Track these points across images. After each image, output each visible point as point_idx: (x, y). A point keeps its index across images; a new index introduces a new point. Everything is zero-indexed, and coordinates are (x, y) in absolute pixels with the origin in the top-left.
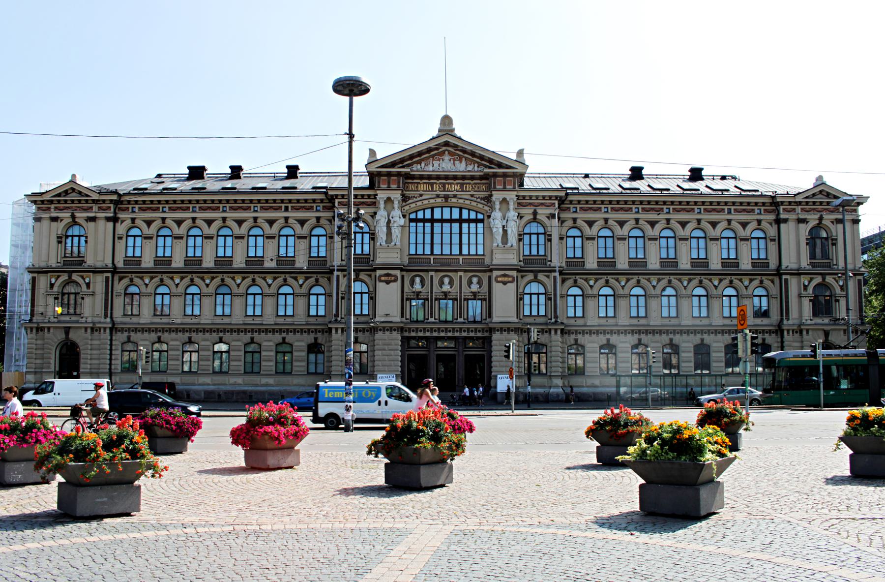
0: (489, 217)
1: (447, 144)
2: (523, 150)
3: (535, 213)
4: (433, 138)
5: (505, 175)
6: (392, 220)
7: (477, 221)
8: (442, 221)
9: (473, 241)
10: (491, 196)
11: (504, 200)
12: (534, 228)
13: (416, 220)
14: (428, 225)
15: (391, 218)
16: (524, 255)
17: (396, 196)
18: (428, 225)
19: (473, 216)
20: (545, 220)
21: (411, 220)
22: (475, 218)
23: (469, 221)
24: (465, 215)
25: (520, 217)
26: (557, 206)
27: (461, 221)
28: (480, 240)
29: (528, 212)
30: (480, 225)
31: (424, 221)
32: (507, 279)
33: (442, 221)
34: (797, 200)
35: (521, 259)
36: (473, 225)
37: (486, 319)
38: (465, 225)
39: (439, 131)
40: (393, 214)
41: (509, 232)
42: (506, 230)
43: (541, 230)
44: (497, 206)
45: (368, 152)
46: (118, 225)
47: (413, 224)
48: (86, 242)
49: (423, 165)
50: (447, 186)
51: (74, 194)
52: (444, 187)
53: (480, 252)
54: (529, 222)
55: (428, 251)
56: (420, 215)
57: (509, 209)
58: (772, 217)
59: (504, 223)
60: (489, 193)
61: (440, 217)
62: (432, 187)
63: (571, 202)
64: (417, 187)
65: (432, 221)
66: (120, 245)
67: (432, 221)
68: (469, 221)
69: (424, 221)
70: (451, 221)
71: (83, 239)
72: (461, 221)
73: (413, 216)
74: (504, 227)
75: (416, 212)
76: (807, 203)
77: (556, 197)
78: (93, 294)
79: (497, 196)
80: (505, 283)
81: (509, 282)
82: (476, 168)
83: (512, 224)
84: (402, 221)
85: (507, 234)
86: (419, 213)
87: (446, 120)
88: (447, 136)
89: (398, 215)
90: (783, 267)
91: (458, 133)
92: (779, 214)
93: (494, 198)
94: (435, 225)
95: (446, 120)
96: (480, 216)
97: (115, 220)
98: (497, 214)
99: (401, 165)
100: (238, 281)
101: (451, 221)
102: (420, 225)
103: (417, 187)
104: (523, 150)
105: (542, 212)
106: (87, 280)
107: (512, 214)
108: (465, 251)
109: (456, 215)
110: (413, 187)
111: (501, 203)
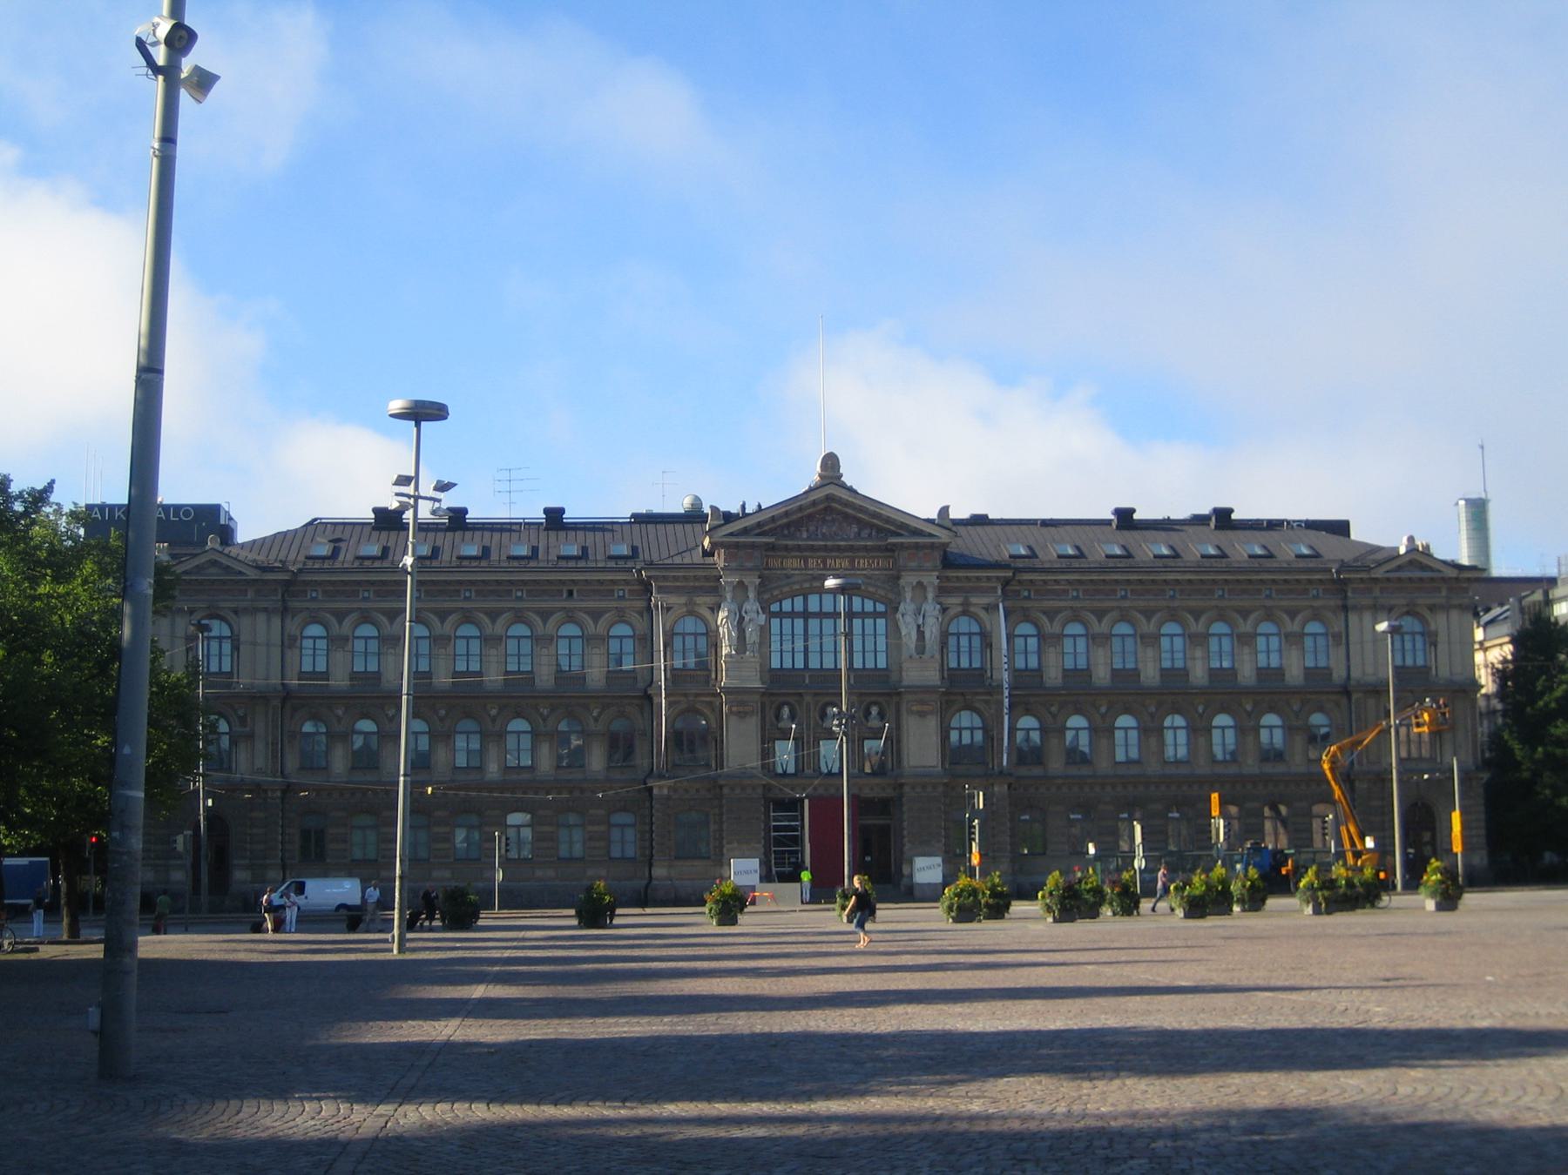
0: (897, 609)
1: (829, 498)
3: (966, 604)
4: (811, 490)
5: (917, 546)
6: (747, 618)
7: (875, 615)
8: (821, 615)
9: (869, 646)
10: (898, 578)
11: (920, 584)
12: (964, 624)
13: (781, 615)
15: (743, 614)
16: (949, 669)
17: (752, 581)
18: (799, 623)
19: (869, 606)
20: (983, 614)
21: (773, 615)
22: (872, 609)
23: (863, 615)
25: (944, 610)
26: (999, 592)
28: (881, 646)
29: (954, 601)
30: (881, 622)
31: (792, 615)
32: (926, 708)
33: (821, 615)
34: (1373, 576)
35: (946, 676)
36: (869, 622)
37: (892, 769)
38: (857, 622)
40: (747, 606)
41: (927, 635)
42: (923, 632)
43: (976, 629)
44: (908, 595)
46: (288, 621)
47: (775, 622)
48: (236, 648)
49: (792, 529)
50: (828, 561)
51: (213, 570)
52: (824, 563)
53: (882, 664)
54: (957, 616)
55: (800, 664)
57: (926, 598)
58: (1334, 602)
59: (920, 621)
60: (894, 572)
61: (817, 610)
62: (806, 562)
63: (1020, 582)
64: (782, 563)
65: (806, 615)
66: (292, 656)
67: (806, 615)
68: (863, 615)
69: (792, 615)
71: (227, 647)
73: (775, 607)
74: (919, 626)
76: (1388, 580)
77: (998, 578)
78: (251, 736)
79: (908, 580)
80: (922, 715)
83: (931, 621)
84: (762, 618)
85: (924, 637)
87: (831, 463)
88: (832, 486)
89: (755, 608)
90: (1353, 682)
91: (848, 479)
92: (1346, 597)
93: (902, 582)
94: (811, 621)
95: (831, 463)
96: (881, 608)
97: (285, 611)
98: (907, 607)
99: (757, 531)
100: (494, 712)
102: (787, 622)
103: (782, 563)
105: (978, 600)
106: (241, 713)
107: (931, 608)
110: (777, 563)
111: (913, 588)
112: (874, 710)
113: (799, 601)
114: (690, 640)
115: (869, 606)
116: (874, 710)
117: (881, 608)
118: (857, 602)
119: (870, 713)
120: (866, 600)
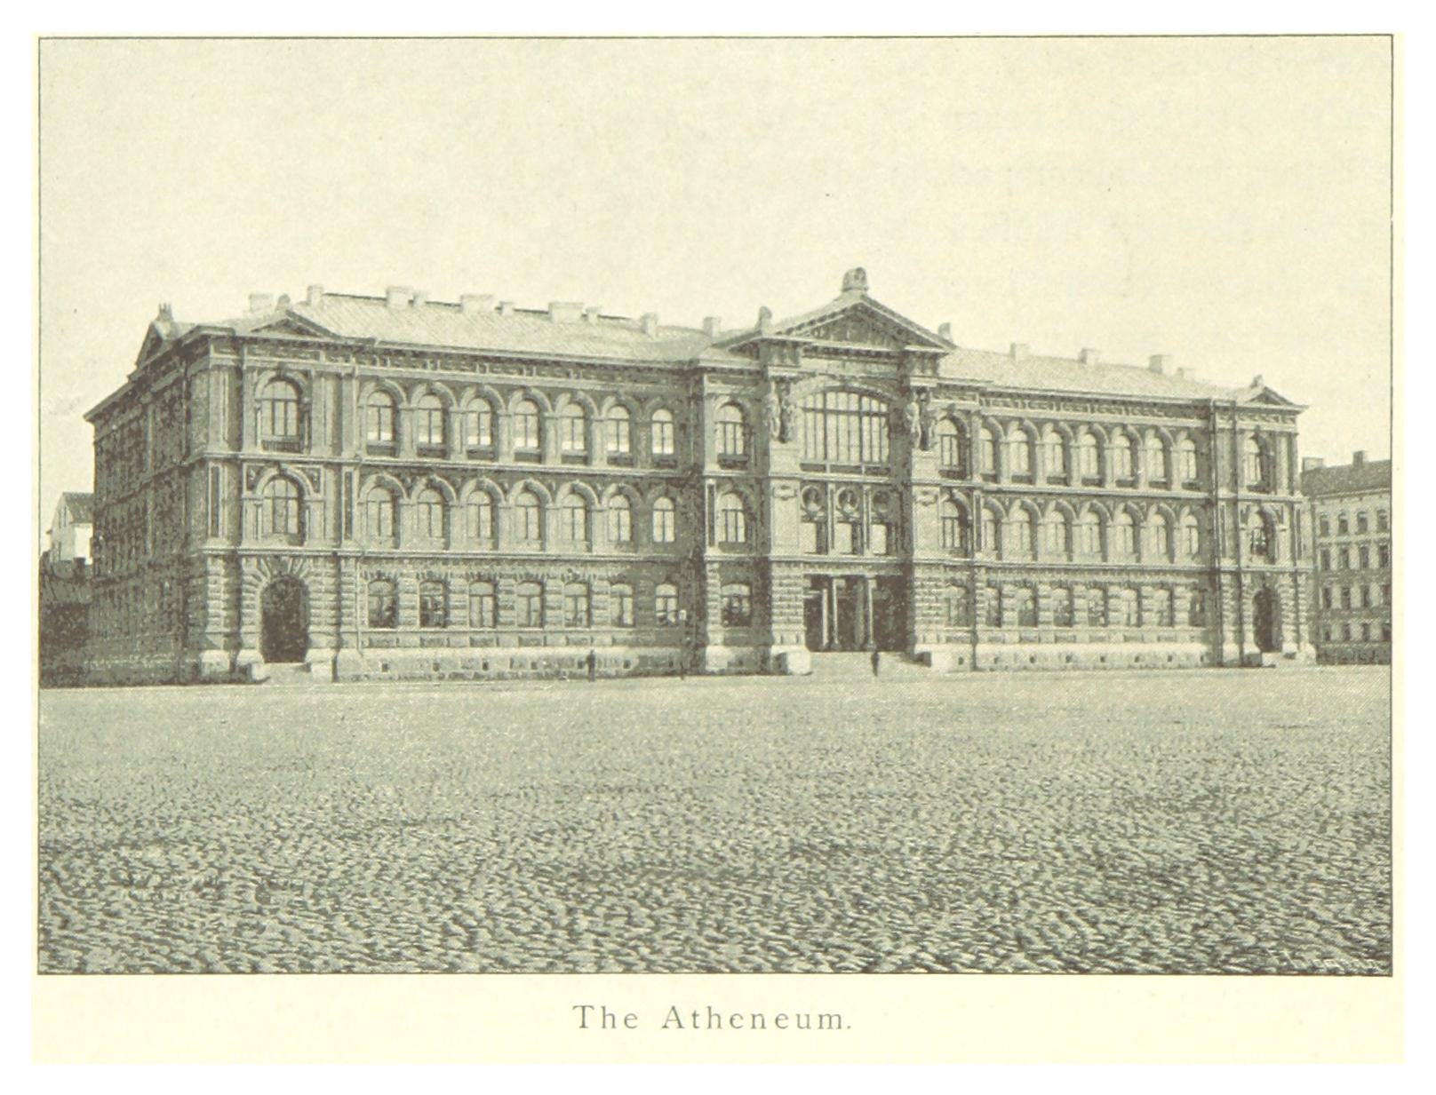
5: (923, 355)
7: (878, 414)
23: (870, 414)
24: (865, 408)
27: (860, 414)
67: (825, 412)
70: (848, 413)
72: (860, 414)
96: (884, 408)
101: (848, 413)
108: (866, 457)
109: (854, 407)
113: (820, 397)
115: (875, 405)
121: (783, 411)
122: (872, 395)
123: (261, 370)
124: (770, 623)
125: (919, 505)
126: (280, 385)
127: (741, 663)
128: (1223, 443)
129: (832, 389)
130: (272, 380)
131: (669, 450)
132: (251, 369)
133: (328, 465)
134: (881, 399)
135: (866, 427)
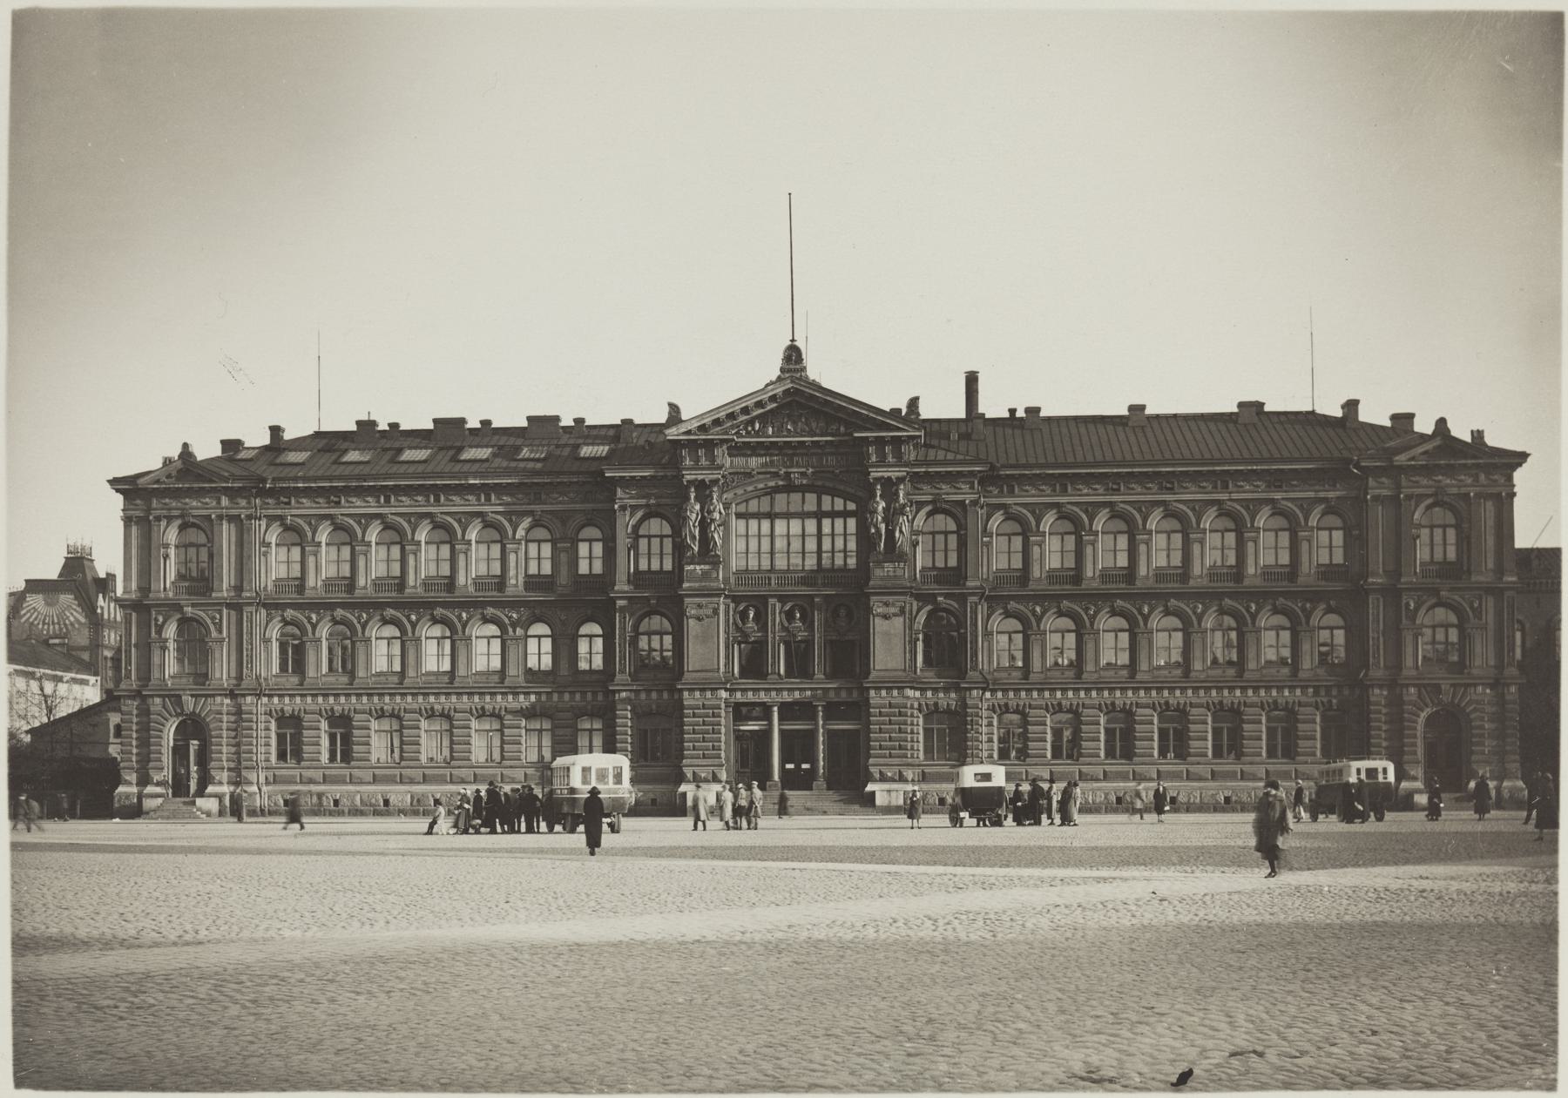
2: (917, 399)
7: (845, 514)
14: (766, 525)
22: (841, 508)
23: (833, 515)
24: (826, 506)
28: (852, 545)
36: (839, 522)
38: (826, 523)
39: (782, 370)
45: (667, 409)
56: (753, 506)
72: (819, 515)
75: (747, 501)
81: (895, 615)
82: (842, 429)
86: (751, 502)
87: (793, 355)
91: (813, 373)
95: (793, 355)
96: (852, 506)
101: (803, 516)
104: (917, 399)
108: (826, 562)
109: (813, 508)
112: (843, 612)
114: (656, 542)
115: (839, 504)
116: (843, 612)
117: (852, 506)
118: (826, 500)
119: (838, 616)
120: (836, 499)
121: (703, 518)
122: (834, 493)
123: (1420, 498)
124: (683, 757)
125: (878, 621)
126: (940, 517)
127: (654, 801)
128: (1379, 516)
129: (776, 490)
130: (1429, 507)
131: (547, 569)
132: (1409, 497)
133: (1489, 590)
134: (846, 497)
135: (826, 529)
